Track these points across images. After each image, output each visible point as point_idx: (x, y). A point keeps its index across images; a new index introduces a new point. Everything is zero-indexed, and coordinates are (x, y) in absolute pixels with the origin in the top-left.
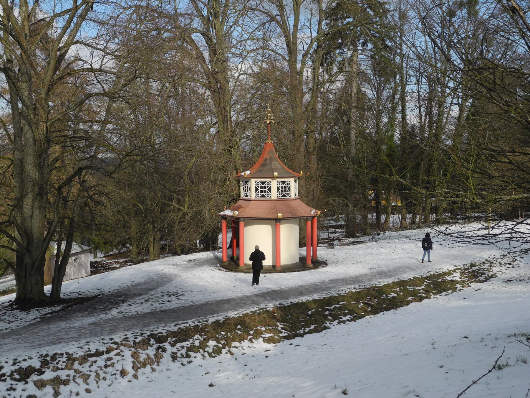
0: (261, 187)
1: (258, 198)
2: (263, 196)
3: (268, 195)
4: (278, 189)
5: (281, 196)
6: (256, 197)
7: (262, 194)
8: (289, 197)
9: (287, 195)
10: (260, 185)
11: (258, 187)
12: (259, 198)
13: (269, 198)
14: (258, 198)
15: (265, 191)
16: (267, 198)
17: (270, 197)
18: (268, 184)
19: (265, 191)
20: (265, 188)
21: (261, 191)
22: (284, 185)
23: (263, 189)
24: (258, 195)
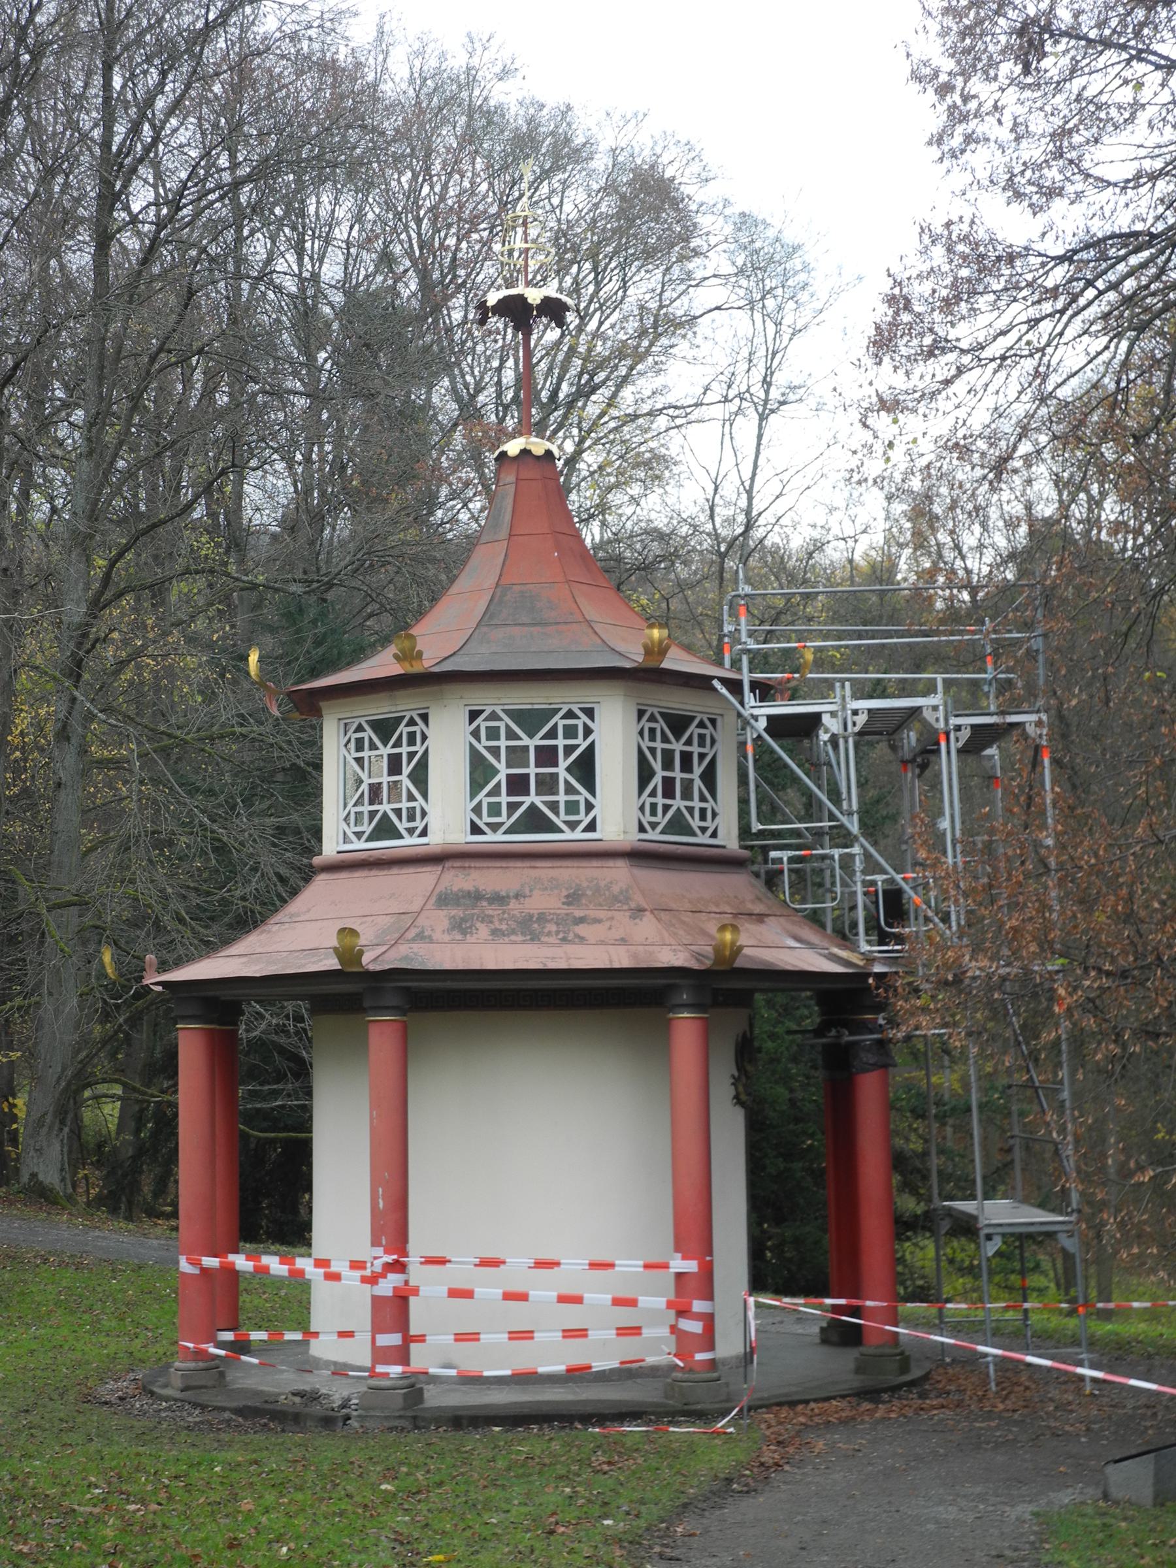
0: (517, 755)
1: (490, 837)
2: (535, 821)
3: (572, 807)
4: (645, 774)
5: (663, 820)
6: (475, 830)
7: (527, 801)
8: (704, 839)
9: (695, 823)
10: (511, 735)
11: (495, 751)
12: (499, 837)
13: (578, 834)
14: (490, 837)
15: (547, 785)
16: (568, 835)
17: (591, 827)
18: (570, 732)
19: (547, 785)
20: (547, 756)
21: (518, 785)
22: (678, 747)
23: (532, 770)
24: (495, 810)
